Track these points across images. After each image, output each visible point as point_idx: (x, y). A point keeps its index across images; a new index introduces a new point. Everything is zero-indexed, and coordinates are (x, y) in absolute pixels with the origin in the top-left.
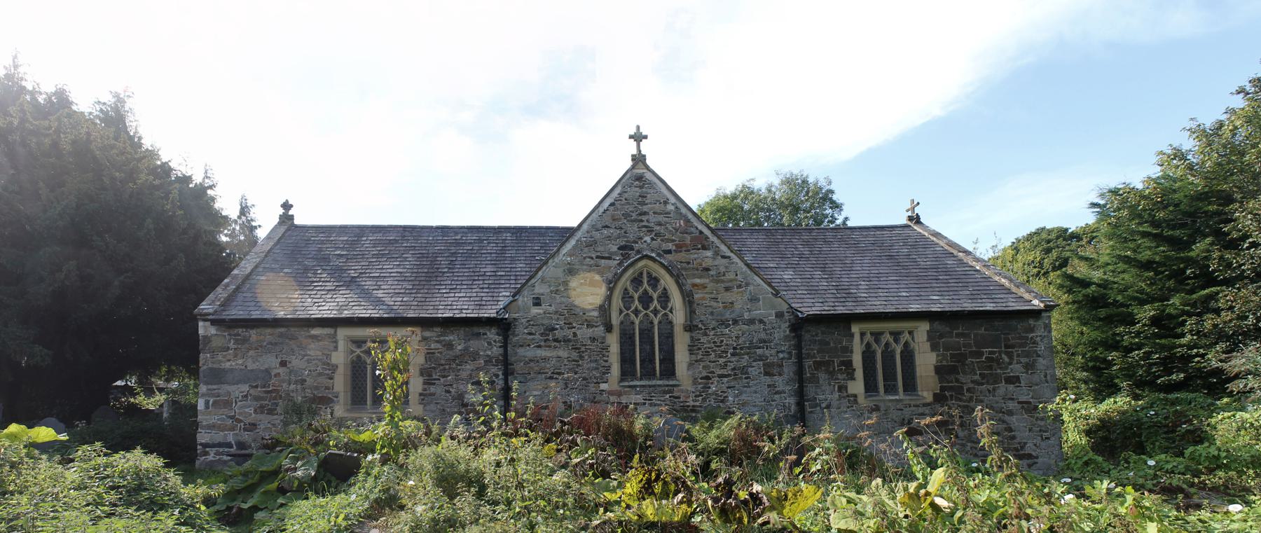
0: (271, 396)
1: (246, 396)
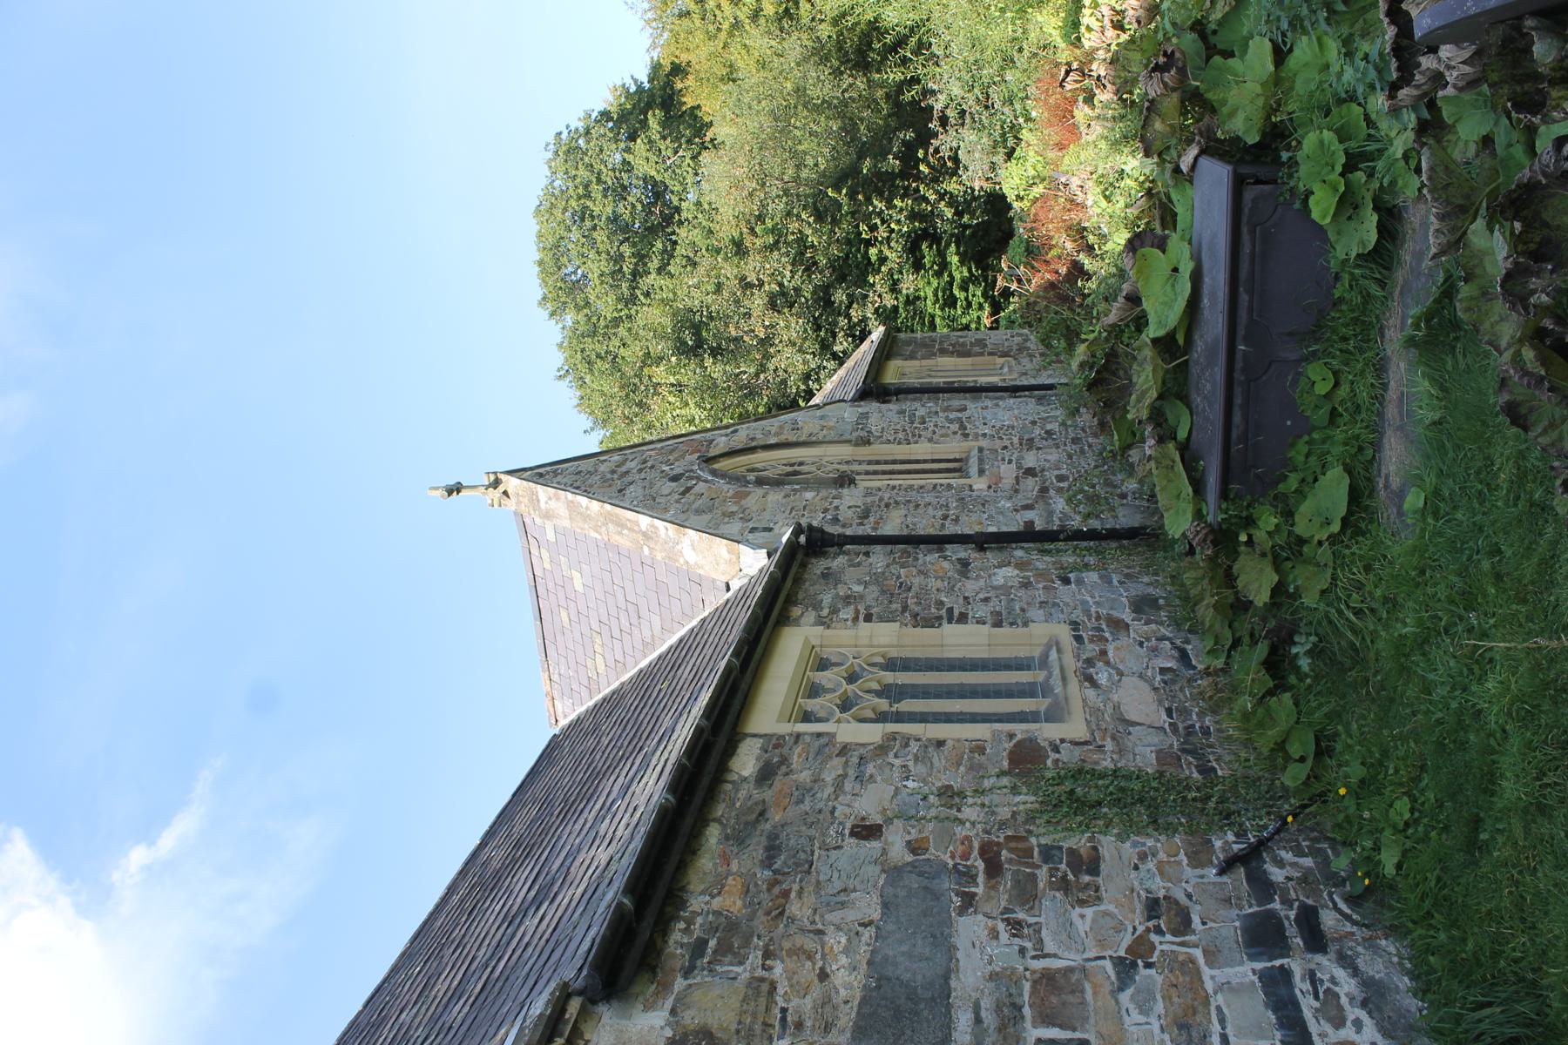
0: (1010, 861)
1: (1016, 927)
